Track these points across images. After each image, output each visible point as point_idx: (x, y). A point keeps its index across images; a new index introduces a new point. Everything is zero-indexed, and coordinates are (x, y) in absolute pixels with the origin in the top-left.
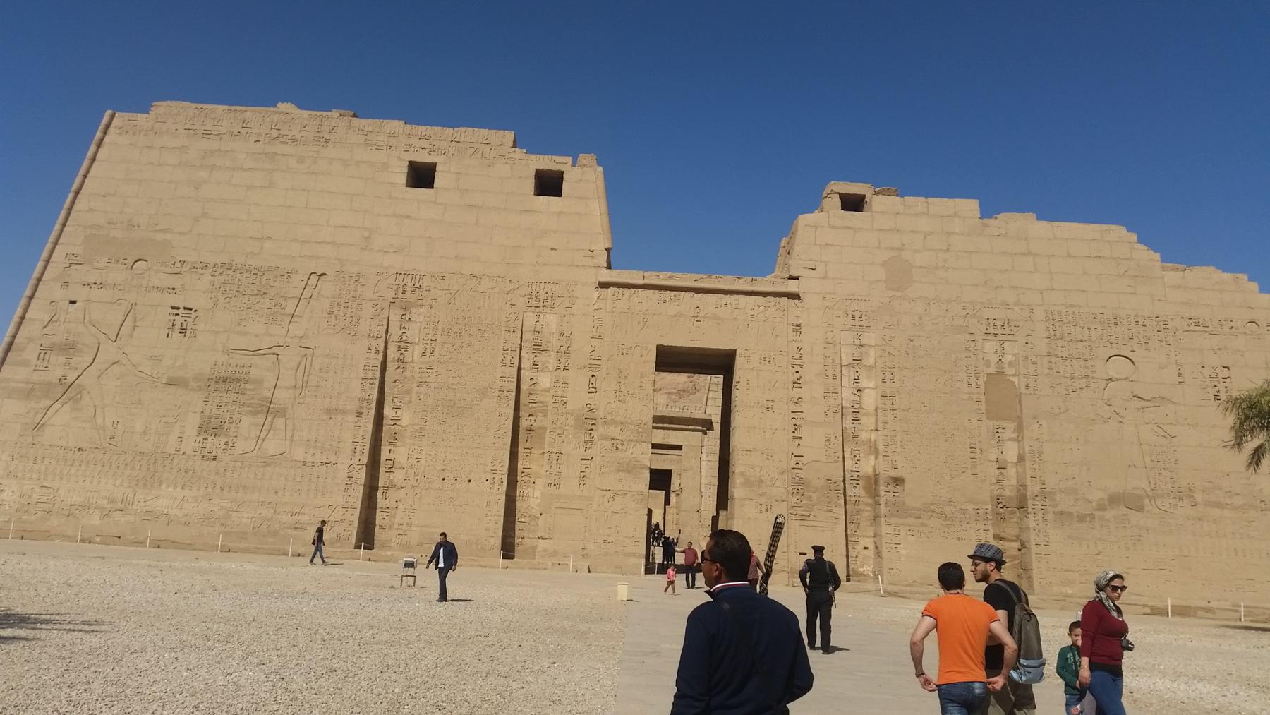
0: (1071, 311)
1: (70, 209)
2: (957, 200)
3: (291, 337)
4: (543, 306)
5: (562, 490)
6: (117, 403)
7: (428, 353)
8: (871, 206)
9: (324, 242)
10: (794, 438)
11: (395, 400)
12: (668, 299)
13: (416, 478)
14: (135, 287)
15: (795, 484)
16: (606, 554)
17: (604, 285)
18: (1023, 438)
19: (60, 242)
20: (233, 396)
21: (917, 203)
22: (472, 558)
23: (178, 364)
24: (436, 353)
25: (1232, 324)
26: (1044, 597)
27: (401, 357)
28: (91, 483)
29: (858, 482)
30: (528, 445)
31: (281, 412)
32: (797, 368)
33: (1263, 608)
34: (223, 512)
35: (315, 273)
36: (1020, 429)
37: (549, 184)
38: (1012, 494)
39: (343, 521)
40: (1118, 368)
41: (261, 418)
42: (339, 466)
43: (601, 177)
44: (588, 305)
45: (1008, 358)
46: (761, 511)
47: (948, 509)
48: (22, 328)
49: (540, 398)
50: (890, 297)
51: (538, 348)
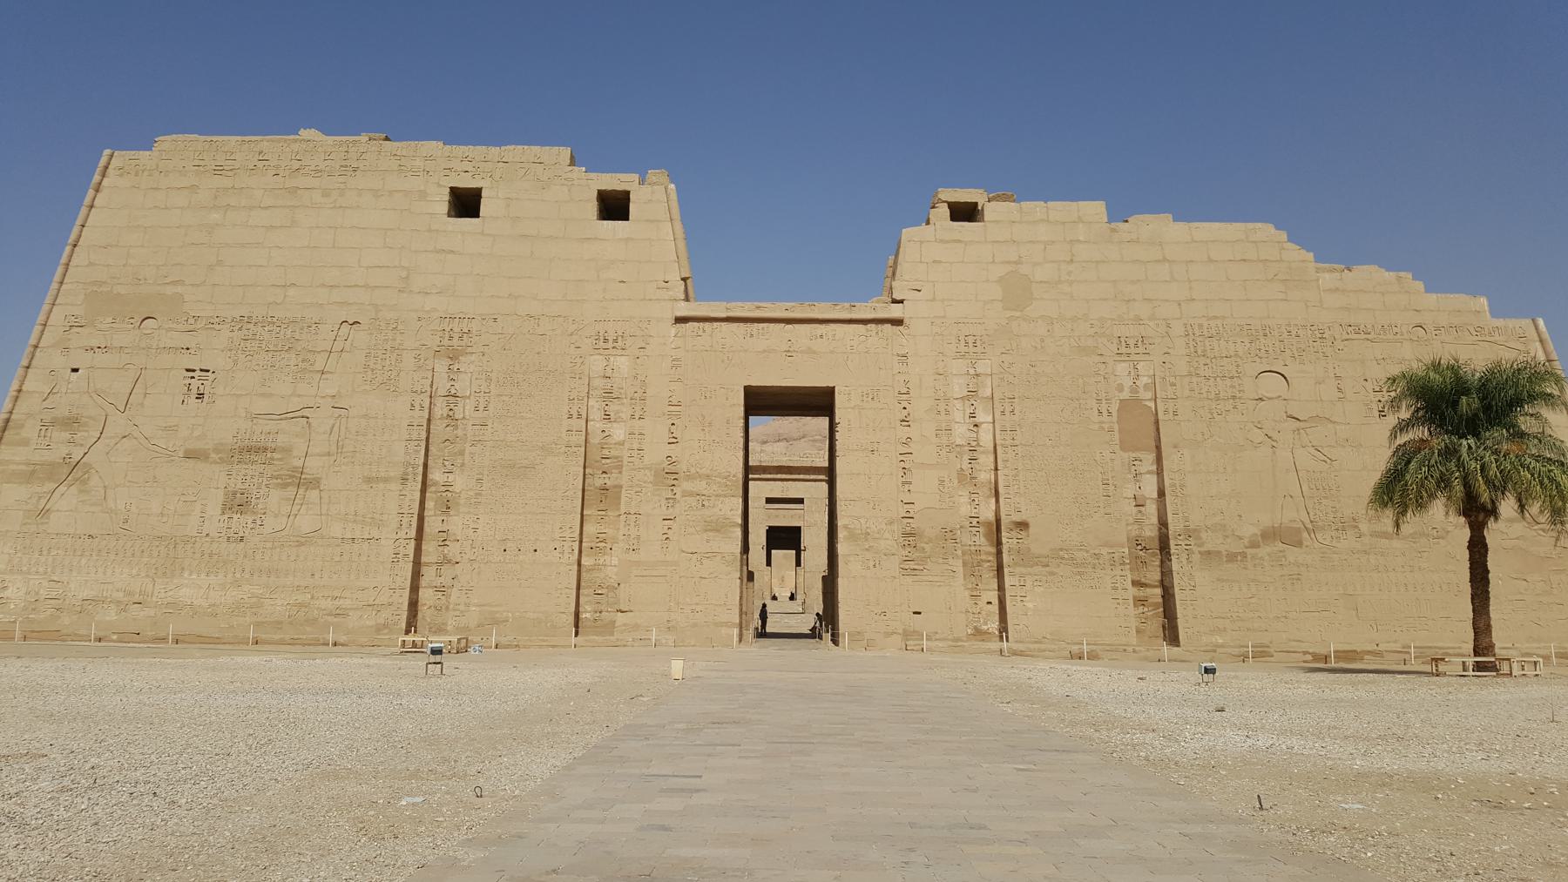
2: (1080, 202)
3: (324, 397)
4: (613, 348)
6: (129, 481)
7: (481, 408)
8: (983, 215)
9: (356, 286)
10: (904, 483)
11: (446, 463)
12: (754, 333)
13: (474, 550)
14: (144, 349)
15: (907, 535)
16: (695, 625)
17: (680, 320)
18: (1162, 470)
19: (58, 301)
20: (260, 468)
21: (1036, 208)
22: (541, 638)
23: (196, 433)
24: (491, 408)
25: (1395, 330)
26: (1191, 649)
27: (451, 413)
28: (104, 573)
29: (977, 529)
30: (602, 506)
31: (314, 483)
32: (905, 404)
33: (1435, 647)
34: (254, 600)
35: (346, 322)
36: (1159, 460)
37: (614, 207)
38: (1153, 535)
40: (1272, 384)
41: (291, 491)
42: (383, 542)
43: (674, 196)
44: (665, 344)
45: (1145, 380)
46: (868, 568)
47: (1079, 555)
48: (18, 403)
49: (614, 453)
50: (1007, 318)
51: (609, 395)
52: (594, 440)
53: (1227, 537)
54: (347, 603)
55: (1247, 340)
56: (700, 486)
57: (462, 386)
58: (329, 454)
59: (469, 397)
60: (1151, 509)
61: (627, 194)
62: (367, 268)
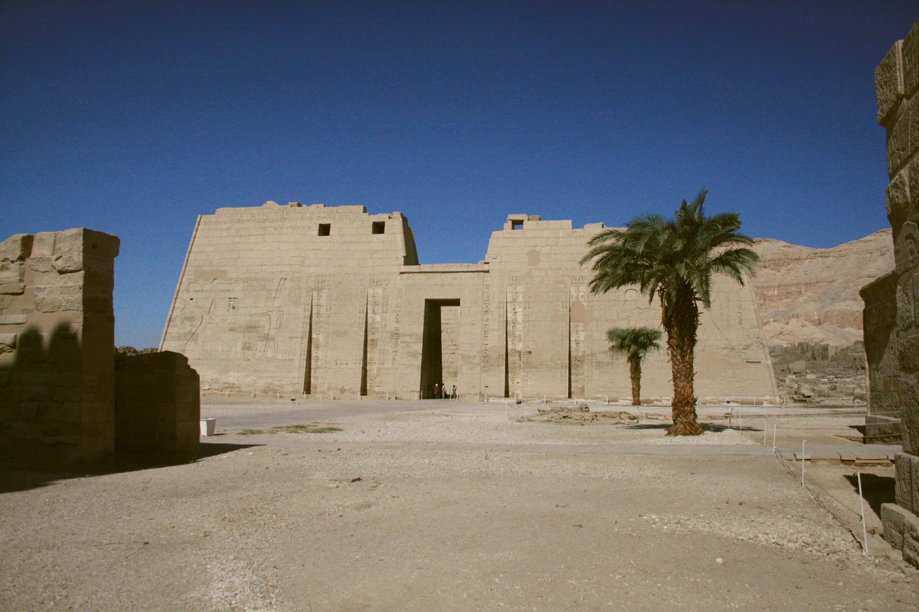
1: (188, 260)
5: (386, 366)
7: (329, 309)
10: (485, 337)
17: (402, 273)
19: (185, 274)
20: (253, 334)
31: (273, 339)
32: (487, 305)
37: (379, 228)
39: (298, 383)
41: (264, 343)
42: (295, 361)
45: (581, 294)
49: (376, 326)
51: (375, 304)
54: (284, 383)
56: (407, 339)
57: (323, 302)
59: (325, 306)
61: (384, 223)
62: (290, 257)
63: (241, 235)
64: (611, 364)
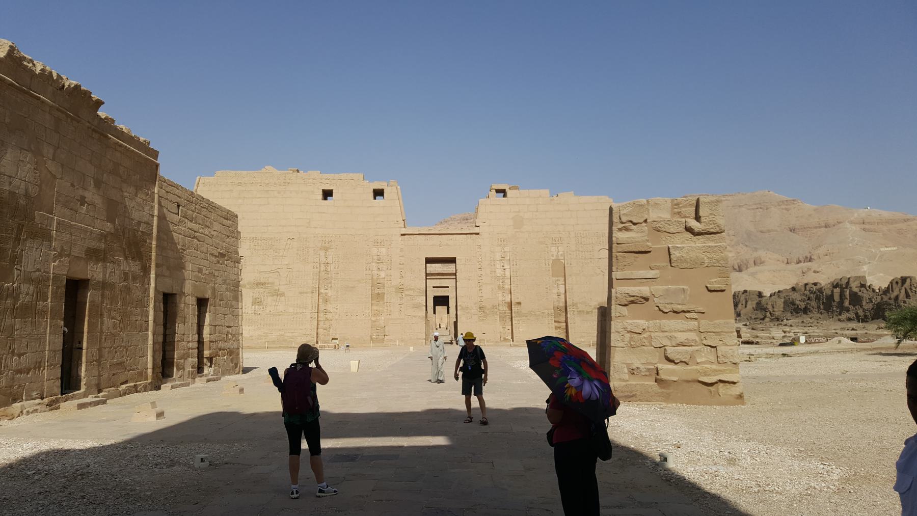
0: (585, 232)
7: (336, 267)
10: (480, 290)
12: (428, 239)
17: (402, 235)
31: (283, 295)
32: (480, 263)
37: (378, 193)
41: (275, 297)
42: (307, 314)
43: (399, 191)
45: (561, 253)
47: (537, 313)
49: (381, 282)
52: (375, 277)
53: (586, 306)
55: (596, 238)
56: (411, 293)
57: (330, 260)
58: (287, 284)
60: (563, 296)
63: (244, 197)
64: (590, 313)
